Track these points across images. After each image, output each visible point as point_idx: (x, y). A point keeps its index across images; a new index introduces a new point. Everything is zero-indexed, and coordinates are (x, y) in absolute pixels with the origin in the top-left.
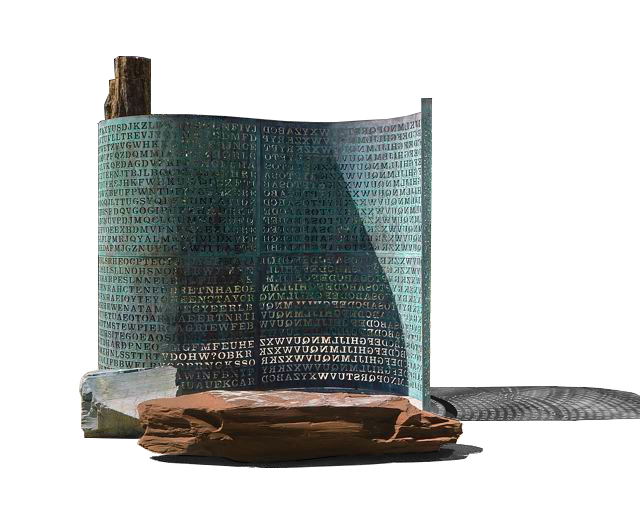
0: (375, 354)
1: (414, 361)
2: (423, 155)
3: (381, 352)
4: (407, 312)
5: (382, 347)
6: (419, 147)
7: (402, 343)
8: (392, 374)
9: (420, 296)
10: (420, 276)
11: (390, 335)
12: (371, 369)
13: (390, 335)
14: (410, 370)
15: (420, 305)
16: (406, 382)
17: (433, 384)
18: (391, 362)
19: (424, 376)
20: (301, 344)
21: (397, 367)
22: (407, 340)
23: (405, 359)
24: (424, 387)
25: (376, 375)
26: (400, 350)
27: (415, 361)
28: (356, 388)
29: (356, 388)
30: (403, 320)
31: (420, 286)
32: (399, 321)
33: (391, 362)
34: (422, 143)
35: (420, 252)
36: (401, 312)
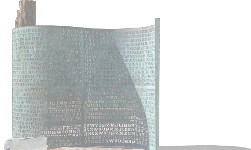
0: (134, 131)
1: (152, 134)
2: (156, 44)
3: (137, 130)
4: (149, 113)
5: (138, 128)
6: (154, 40)
7: (146, 127)
8: (142, 140)
9: (154, 106)
10: (154, 97)
11: (141, 123)
12: (133, 138)
13: (141, 123)
14: (150, 138)
15: (154, 110)
16: (148, 144)
17: (160, 144)
18: (142, 135)
19: (156, 141)
20: (90, 116)
21: (144, 137)
22: (149, 125)
23: (148, 134)
24: (156, 146)
25: (135, 141)
26: (146, 130)
27: (152, 134)
28: (126, 146)
29: (126, 146)
30: (147, 116)
31: (154, 101)
32: (145, 117)
33: (142, 135)
34: (155, 38)
35: (154, 87)
36: (146, 113)
